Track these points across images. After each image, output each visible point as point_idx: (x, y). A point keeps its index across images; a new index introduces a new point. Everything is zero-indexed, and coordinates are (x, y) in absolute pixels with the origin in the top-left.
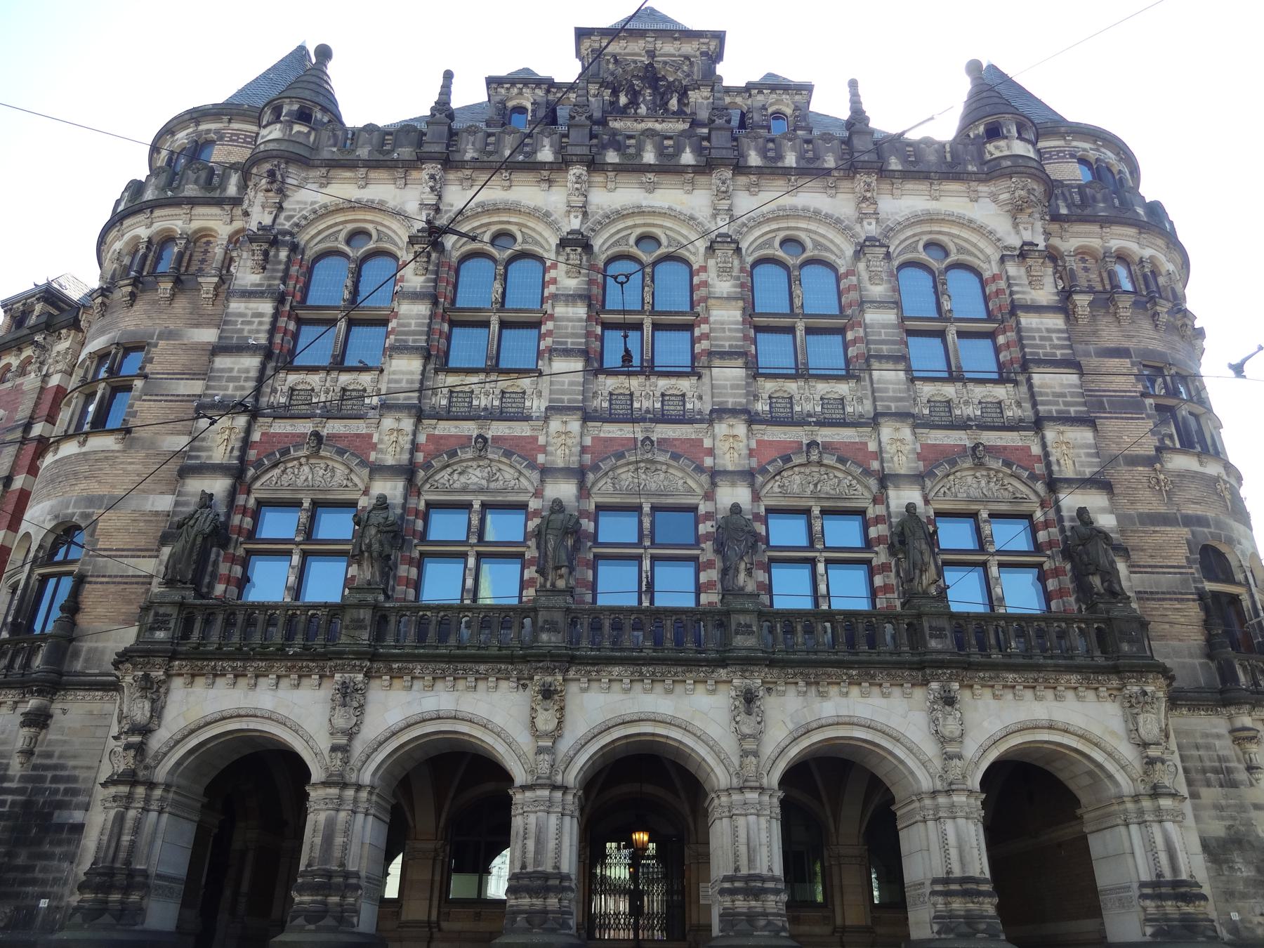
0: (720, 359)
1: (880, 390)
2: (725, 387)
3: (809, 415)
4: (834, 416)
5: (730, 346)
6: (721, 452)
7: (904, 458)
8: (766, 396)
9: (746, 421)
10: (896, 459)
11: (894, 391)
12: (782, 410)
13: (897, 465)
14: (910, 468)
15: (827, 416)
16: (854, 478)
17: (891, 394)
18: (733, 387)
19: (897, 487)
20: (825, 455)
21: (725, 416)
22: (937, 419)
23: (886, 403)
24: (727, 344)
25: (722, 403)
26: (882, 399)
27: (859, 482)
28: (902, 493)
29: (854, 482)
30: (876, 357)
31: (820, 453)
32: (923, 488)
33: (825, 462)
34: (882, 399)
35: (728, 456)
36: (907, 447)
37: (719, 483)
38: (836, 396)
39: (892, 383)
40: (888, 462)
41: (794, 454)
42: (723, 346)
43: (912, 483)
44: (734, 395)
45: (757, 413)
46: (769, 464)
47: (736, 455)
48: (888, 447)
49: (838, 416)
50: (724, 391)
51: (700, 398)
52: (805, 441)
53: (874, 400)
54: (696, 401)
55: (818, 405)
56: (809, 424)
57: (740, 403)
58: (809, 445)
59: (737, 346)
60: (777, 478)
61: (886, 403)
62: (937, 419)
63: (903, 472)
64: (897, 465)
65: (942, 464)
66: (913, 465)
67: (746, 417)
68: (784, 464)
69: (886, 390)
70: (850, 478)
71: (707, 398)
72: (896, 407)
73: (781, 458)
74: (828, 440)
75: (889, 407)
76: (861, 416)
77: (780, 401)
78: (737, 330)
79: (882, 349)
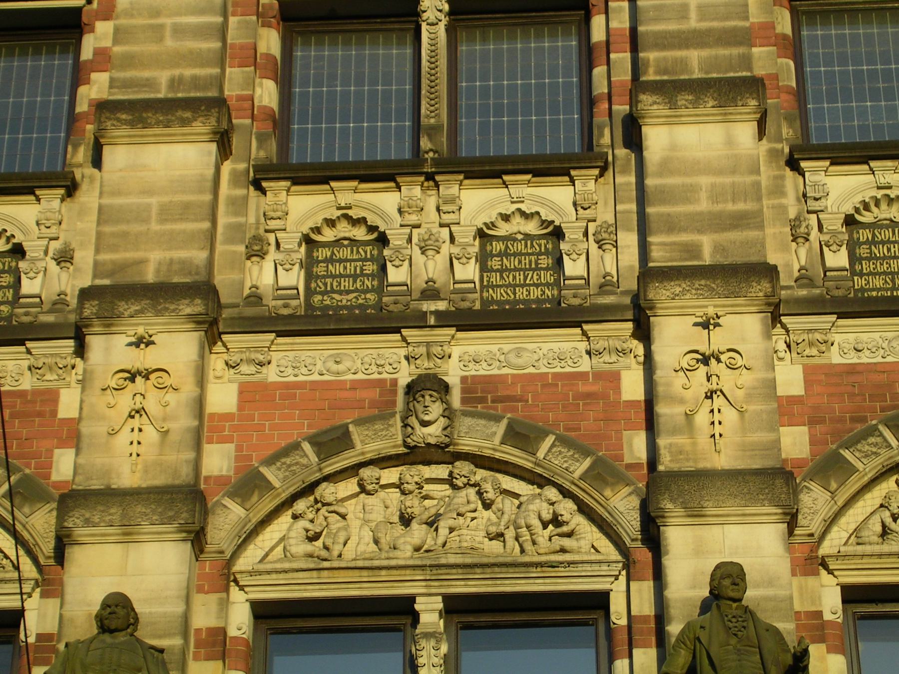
0: (132, 124)
1: (667, 196)
2: (141, 215)
3: (431, 293)
4: (521, 293)
5: (174, 83)
6: (102, 429)
7: (730, 416)
8: (291, 240)
9: (197, 320)
10: (702, 418)
11: (716, 195)
12: (346, 284)
13: (703, 440)
14: (744, 448)
15: (497, 295)
16: (566, 493)
17: (703, 205)
18: (166, 214)
19: (695, 513)
20: (468, 421)
21: (127, 308)
22: (878, 282)
23: (684, 238)
24: (163, 77)
25: (122, 267)
26: (671, 225)
27: (584, 509)
28: (715, 532)
29: (566, 508)
30: (658, 88)
31: (449, 414)
32: (792, 521)
33: (467, 443)
34: (671, 225)
35: (124, 437)
36: (746, 378)
37: (81, 533)
38: (532, 227)
39: (707, 169)
40: (675, 431)
41: (359, 422)
42: (149, 84)
43: (753, 500)
44: (171, 240)
45: (255, 298)
46: (270, 461)
47: (151, 434)
48: (680, 380)
49: (536, 293)
50: (135, 228)
51: (65, 258)
52: (404, 379)
53: (643, 229)
54: (53, 266)
55: (463, 258)
56: (419, 321)
57: (185, 266)
58: (412, 389)
59: (196, 82)
60: (301, 505)
61: (684, 238)
62: (878, 282)
63: (723, 461)
64: (703, 440)
65: (872, 431)
66: (762, 437)
67: (197, 307)
68: (322, 460)
69: (688, 194)
70: (552, 493)
71: (85, 257)
72: (718, 248)
73: (314, 441)
74: (482, 370)
75: (693, 250)
76: (606, 286)
77: (345, 253)
78: (200, 32)
79: (683, 64)
